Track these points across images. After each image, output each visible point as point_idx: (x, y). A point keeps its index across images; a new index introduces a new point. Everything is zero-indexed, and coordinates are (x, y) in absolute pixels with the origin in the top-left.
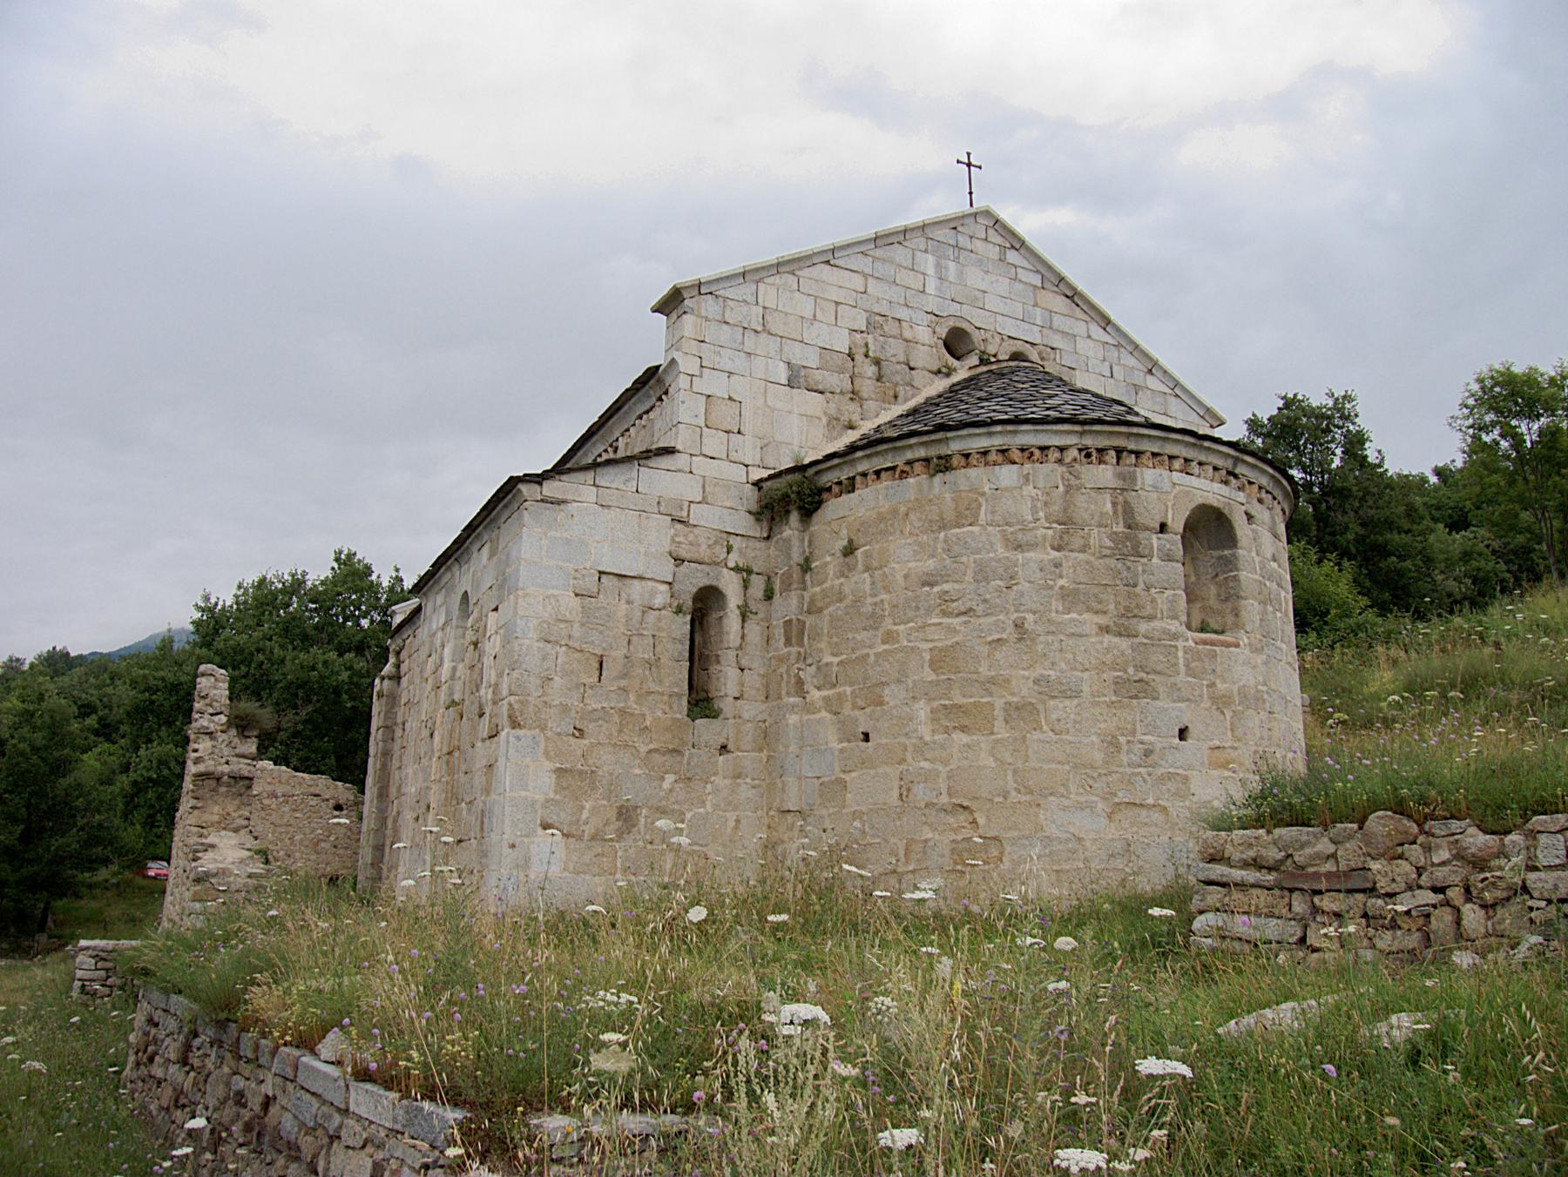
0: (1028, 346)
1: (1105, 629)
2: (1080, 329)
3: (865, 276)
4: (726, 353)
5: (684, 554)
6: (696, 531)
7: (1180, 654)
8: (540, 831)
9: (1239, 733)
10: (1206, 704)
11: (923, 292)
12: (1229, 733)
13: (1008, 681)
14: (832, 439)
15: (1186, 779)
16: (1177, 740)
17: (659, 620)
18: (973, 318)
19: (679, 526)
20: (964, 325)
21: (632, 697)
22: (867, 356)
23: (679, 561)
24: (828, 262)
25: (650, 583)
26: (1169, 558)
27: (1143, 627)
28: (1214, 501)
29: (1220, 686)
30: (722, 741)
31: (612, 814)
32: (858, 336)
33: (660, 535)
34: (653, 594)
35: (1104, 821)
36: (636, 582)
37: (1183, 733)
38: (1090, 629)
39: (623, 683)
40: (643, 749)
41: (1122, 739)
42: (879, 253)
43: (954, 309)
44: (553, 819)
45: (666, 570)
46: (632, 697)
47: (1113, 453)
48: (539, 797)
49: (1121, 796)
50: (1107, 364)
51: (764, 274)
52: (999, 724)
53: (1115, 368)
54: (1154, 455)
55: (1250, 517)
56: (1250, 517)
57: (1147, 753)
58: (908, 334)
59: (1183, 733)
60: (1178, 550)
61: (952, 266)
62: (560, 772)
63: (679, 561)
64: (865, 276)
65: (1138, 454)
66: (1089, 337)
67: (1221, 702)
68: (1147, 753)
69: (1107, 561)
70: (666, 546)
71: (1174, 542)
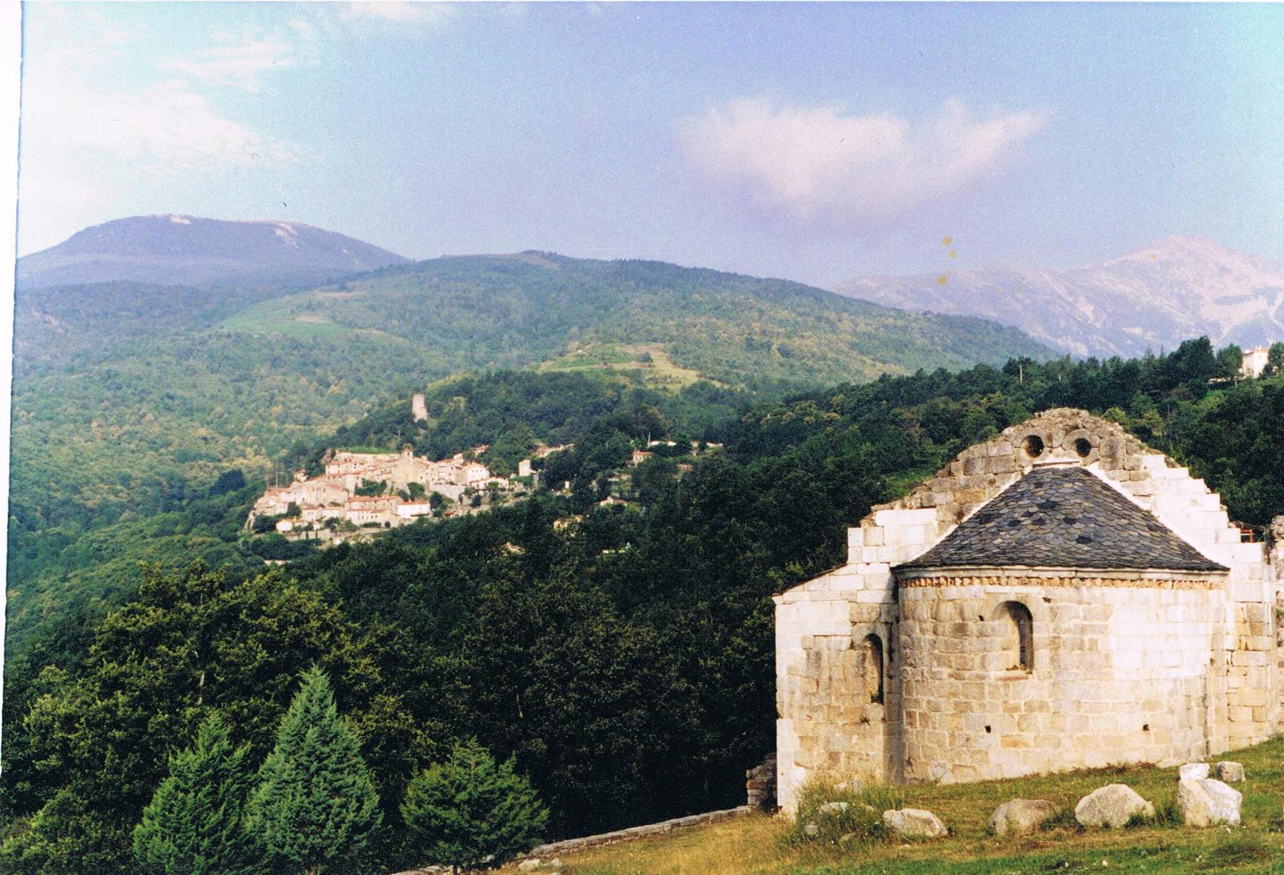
1: (951, 676)
5: (856, 620)
8: (794, 766)
9: (1024, 726)
10: (1001, 712)
12: (1017, 728)
14: (939, 535)
15: (986, 753)
21: (833, 698)
23: (854, 623)
25: (838, 638)
27: (967, 674)
29: (1011, 702)
31: (826, 757)
34: (841, 642)
37: (988, 729)
38: (945, 676)
39: (828, 691)
40: (840, 724)
44: (800, 760)
45: (847, 628)
46: (833, 698)
48: (793, 751)
49: (957, 762)
57: (967, 740)
62: (801, 738)
65: (971, 578)
68: (967, 740)
70: (848, 616)
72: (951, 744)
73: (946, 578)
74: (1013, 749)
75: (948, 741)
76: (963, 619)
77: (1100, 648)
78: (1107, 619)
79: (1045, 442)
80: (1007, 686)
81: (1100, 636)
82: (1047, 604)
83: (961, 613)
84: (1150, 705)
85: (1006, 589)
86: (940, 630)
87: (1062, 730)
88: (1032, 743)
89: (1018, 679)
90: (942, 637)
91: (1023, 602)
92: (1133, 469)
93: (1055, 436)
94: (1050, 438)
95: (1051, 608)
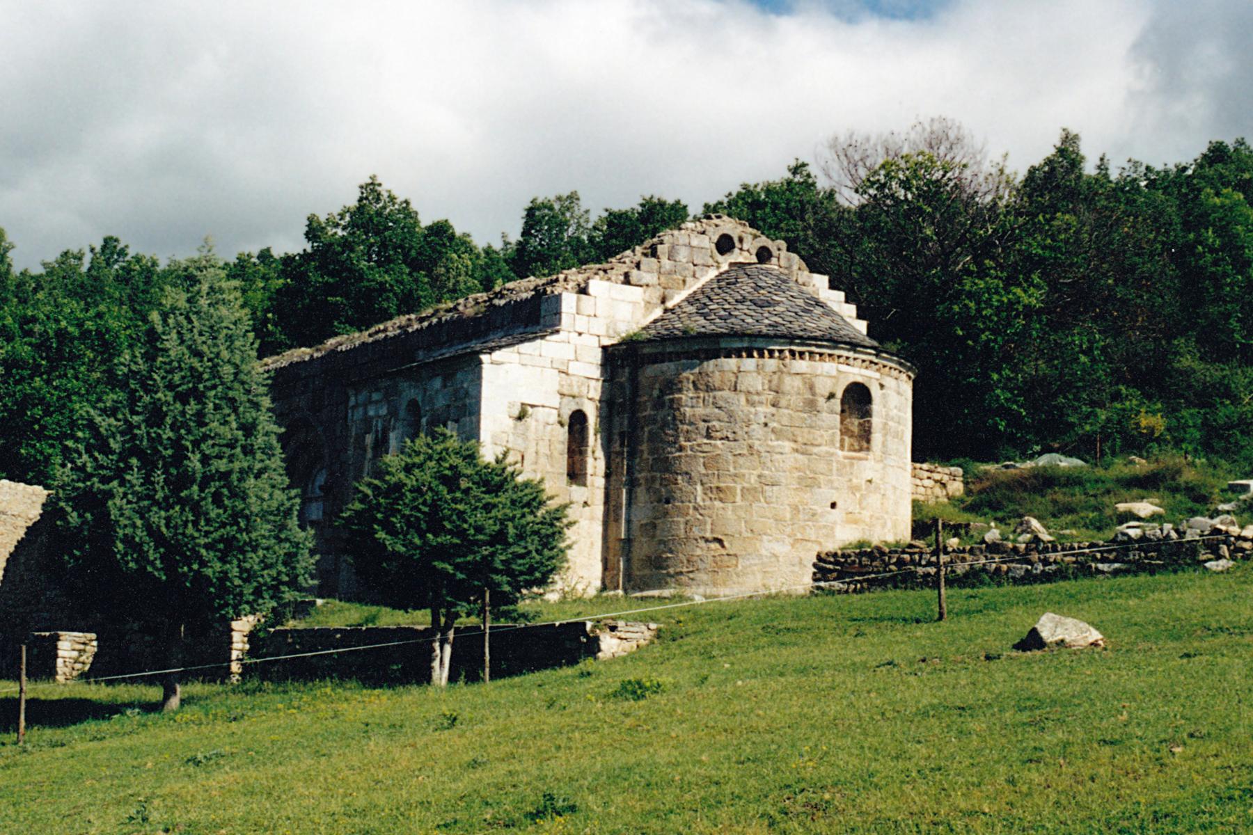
5: (566, 392)
6: (572, 378)
7: (834, 464)
9: (864, 504)
13: (744, 475)
15: (832, 529)
16: (829, 509)
17: (552, 430)
19: (563, 375)
23: (562, 395)
25: (546, 410)
26: (832, 412)
27: (816, 450)
28: (860, 379)
29: (855, 481)
30: (584, 499)
33: (553, 382)
34: (549, 415)
35: (790, 548)
36: (540, 409)
37: (833, 505)
38: (787, 450)
41: (801, 508)
45: (555, 401)
47: (807, 354)
49: (799, 536)
52: (738, 498)
54: (830, 355)
55: (882, 386)
56: (882, 386)
59: (833, 505)
60: (838, 408)
63: (562, 395)
65: (821, 355)
67: (854, 489)
68: (814, 515)
69: (800, 414)
70: (557, 387)
71: (836, 404)
72: (792, 519)
73: (792, 353)
74: (854, 526)
75: (788, 516)
76: (814, 394)
79: (737, 244)
80: (852, 465)
82: (881, 392)
83: (812, 388)
85: (855, 370)
86: (783, 402)
89: (860, 459)
90: (786, 411)
91: (867, 384)
92: (804, 285)
93: (745, 240)
94: (741, 240)
95: (884, 394)
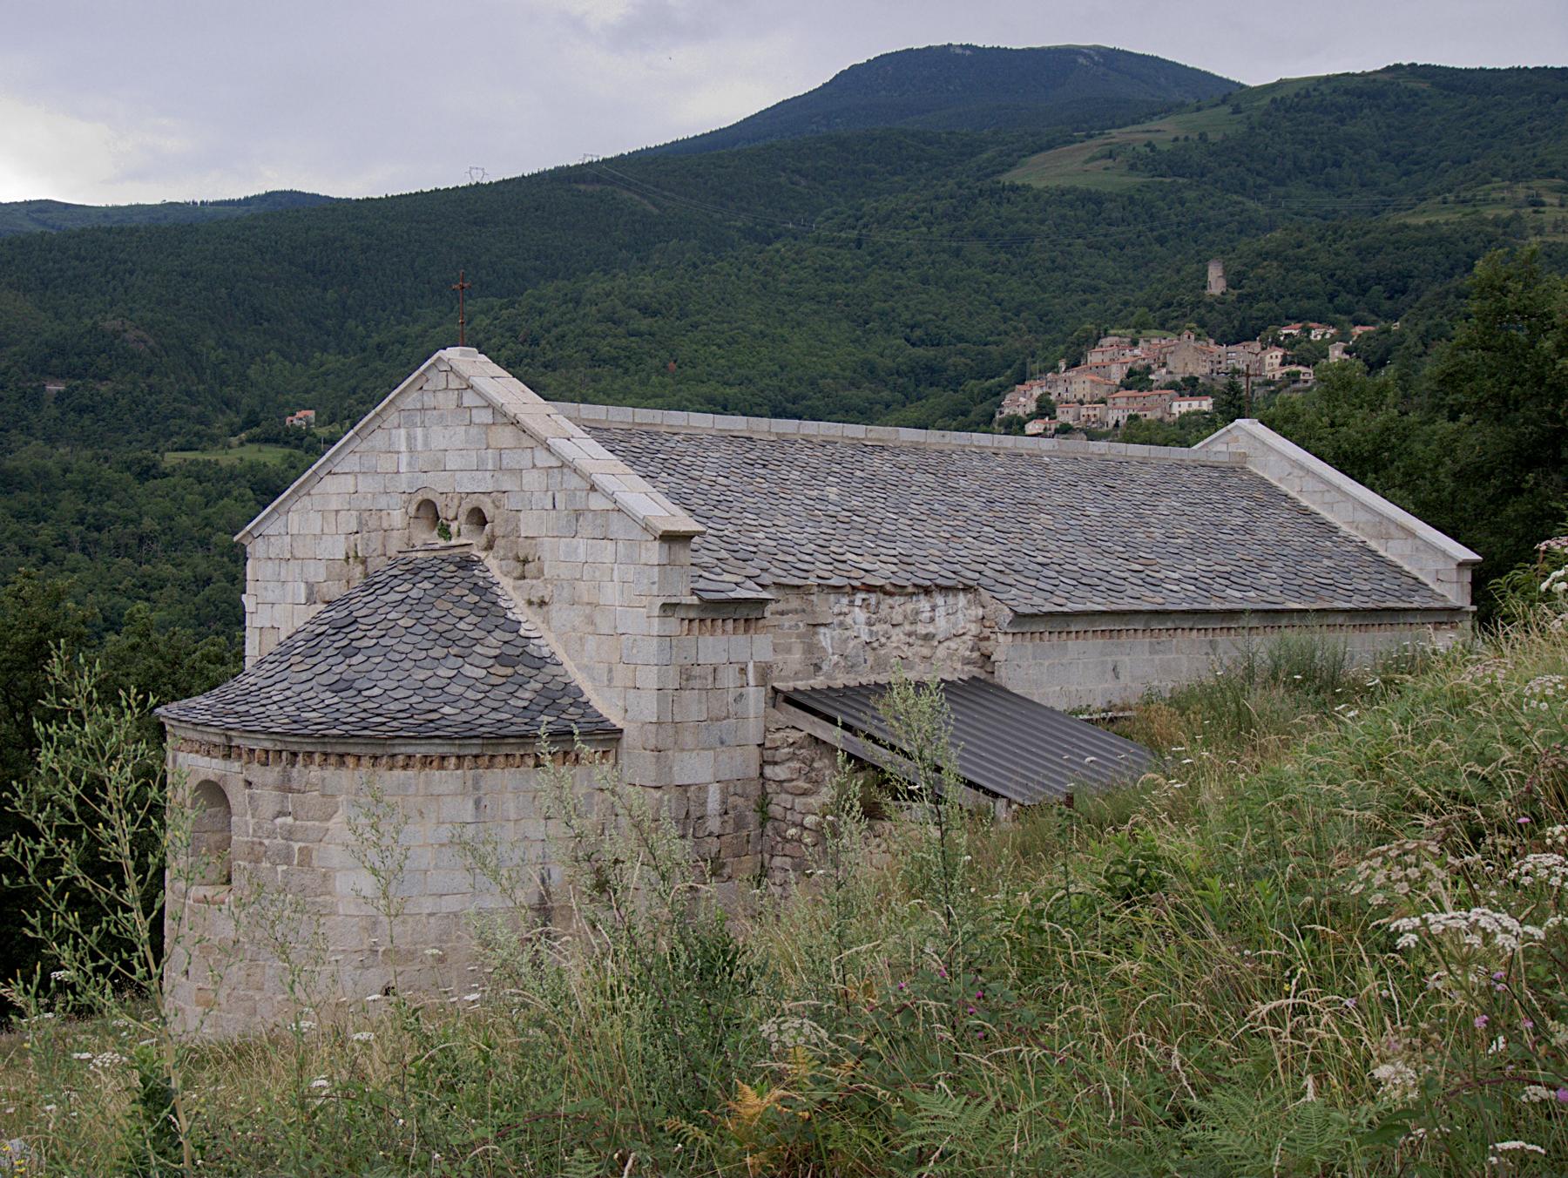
0: (482, 496)
2: (525, 459)
3: (355, 474)
4: (271, 585)
11: (398, 472)
18: (437, 485)
20: (430, 496)
22: (356, 557)
24: (329, 473)
32: (352, 537)
42: (364, 446)
43: (424, 480)
50: (550, 493)
51: (290, 503)
53: (557, 496)
55: (249, 784)
58: (385, 525)
61: (419, 432)
64: (355, 474)
66: (534, 466)
77: (315, 863)
78: (329, 818)
81: (316, 846)
84: (396, 955)
87: (260, 989)
88: (224, 1005)
